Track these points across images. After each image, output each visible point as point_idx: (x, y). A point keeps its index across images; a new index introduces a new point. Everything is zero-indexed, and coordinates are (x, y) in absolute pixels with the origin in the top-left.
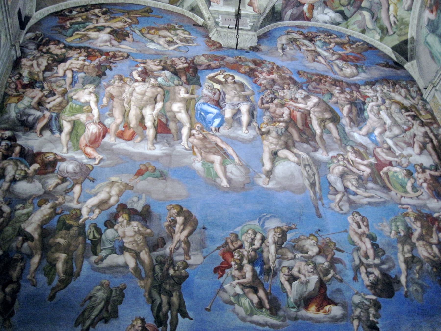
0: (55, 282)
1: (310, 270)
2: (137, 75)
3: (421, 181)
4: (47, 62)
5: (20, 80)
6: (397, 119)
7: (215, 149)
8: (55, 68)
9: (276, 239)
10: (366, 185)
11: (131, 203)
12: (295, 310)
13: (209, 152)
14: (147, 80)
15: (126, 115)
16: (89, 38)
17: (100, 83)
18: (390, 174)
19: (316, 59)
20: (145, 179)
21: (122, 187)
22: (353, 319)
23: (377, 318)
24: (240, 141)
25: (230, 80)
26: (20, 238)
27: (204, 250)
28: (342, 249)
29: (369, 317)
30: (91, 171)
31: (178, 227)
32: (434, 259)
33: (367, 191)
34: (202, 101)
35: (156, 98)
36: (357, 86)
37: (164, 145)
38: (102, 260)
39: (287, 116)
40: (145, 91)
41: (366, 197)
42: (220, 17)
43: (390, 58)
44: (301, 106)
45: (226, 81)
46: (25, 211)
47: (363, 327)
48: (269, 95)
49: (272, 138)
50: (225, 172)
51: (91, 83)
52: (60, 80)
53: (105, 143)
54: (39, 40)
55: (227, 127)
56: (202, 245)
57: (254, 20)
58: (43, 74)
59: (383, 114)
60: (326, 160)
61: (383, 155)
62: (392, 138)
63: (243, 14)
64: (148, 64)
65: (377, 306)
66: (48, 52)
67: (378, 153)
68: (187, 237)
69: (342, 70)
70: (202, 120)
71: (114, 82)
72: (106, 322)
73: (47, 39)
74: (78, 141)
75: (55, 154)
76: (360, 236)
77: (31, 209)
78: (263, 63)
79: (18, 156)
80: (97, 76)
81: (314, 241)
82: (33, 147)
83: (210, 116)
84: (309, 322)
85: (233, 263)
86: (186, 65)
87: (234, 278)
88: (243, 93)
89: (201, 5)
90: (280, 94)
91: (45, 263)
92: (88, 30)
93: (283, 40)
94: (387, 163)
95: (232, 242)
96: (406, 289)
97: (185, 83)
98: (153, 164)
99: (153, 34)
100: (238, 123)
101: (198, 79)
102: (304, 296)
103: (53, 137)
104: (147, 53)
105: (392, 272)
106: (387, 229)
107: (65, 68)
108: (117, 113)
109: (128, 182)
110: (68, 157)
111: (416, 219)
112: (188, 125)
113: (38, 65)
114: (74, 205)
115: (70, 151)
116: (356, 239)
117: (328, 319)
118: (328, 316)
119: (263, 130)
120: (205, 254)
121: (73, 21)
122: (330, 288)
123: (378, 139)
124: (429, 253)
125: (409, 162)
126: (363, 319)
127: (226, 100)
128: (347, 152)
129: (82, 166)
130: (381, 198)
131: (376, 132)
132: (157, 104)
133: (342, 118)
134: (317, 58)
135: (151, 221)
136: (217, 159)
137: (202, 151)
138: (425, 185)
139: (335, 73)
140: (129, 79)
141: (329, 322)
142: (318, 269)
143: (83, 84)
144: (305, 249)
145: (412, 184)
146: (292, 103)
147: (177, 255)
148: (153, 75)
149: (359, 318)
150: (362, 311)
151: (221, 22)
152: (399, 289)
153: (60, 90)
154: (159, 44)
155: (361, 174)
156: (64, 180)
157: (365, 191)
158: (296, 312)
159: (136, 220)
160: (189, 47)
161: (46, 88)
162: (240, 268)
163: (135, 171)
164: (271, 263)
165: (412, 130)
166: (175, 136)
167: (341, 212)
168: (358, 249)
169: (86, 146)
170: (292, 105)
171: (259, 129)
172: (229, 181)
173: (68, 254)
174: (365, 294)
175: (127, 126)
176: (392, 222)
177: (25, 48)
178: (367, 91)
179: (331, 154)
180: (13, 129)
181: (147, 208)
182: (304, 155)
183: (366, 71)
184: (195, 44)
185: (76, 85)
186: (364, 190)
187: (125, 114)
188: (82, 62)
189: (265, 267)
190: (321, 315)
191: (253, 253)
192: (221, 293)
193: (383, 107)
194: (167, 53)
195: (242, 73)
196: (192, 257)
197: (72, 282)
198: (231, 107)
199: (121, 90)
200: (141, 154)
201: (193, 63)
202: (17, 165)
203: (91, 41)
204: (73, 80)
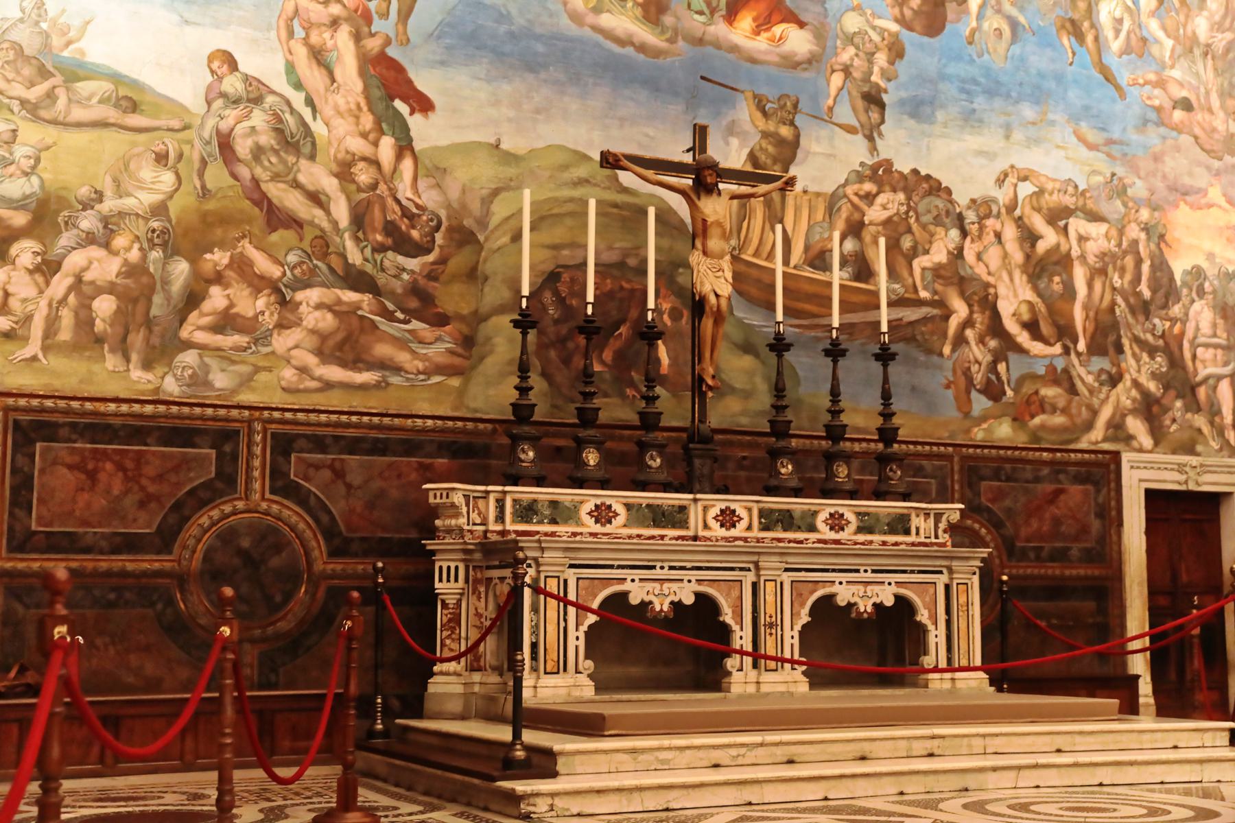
12: (702, 18)
22: (833, 71)
23: (889, 80)
29: (871, 73)
47: (849, 93)
84: (731, 56)
96: (974, 24)
117: (777, 59)
118: (778, 50)
126: (857, 74)
141: (778, 65)
149: (847, 70)
150: (857, 55)
152: (958, 20)
158: (704, 23)
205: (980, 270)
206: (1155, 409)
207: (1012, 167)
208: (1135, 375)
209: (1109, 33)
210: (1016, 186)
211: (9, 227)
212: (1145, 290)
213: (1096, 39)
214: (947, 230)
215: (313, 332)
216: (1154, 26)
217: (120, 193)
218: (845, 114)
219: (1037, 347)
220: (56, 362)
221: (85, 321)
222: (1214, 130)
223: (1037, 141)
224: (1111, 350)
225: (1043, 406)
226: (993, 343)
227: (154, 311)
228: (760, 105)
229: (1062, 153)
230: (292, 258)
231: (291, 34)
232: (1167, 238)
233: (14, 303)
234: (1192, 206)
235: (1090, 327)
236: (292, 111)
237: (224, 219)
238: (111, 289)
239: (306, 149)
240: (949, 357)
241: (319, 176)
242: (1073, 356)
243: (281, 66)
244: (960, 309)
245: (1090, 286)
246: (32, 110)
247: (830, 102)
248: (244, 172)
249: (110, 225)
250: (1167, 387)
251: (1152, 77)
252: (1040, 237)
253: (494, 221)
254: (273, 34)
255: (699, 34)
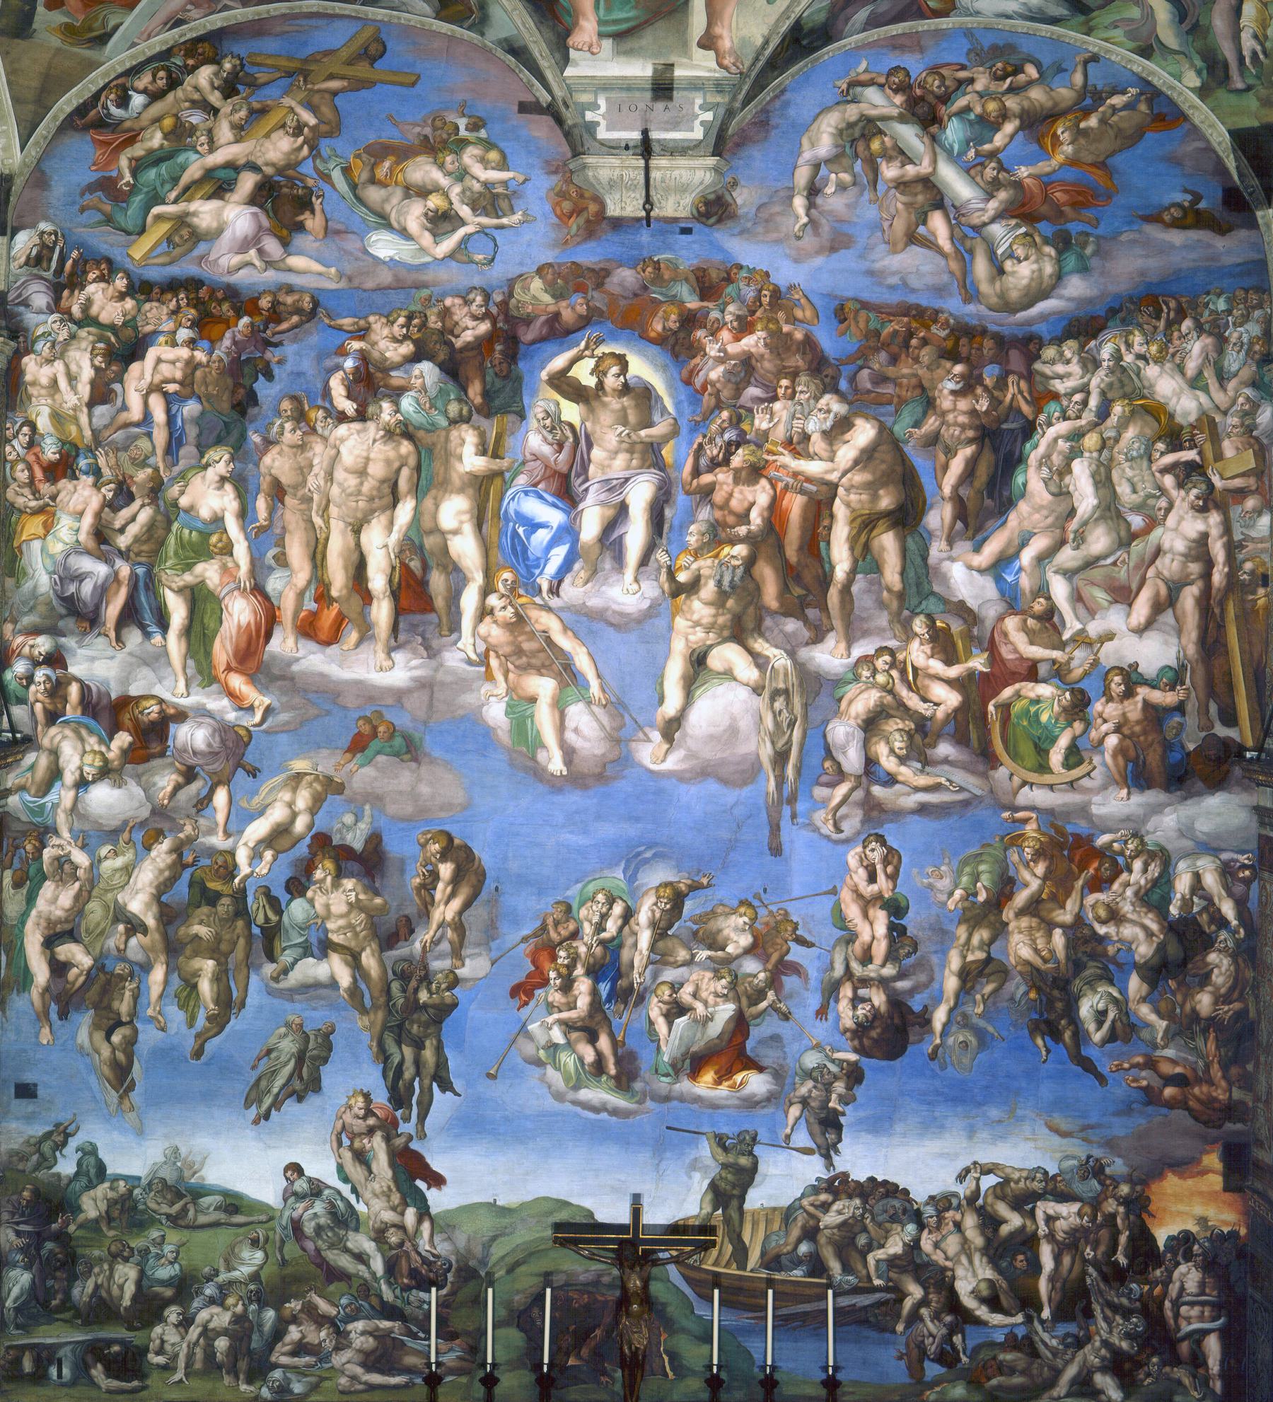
0: (201, 1022)
1: (719, 989)
2: (344, 393)
3: (1105, 728)
4: (93, 365)
5: (37, 450)
6: (1123, 489)
7: (542, 655)
8: (117, 387)
9: (658, 915)
10: (928, 752)
11: (340, 831)
13: (524, 669)
14: (371, 409)
15: (319, 557)
16: (197, 236)
17: (243, 437)
18: (1017, 708)
19: (921, 229)
20: (370, 762)
21: (318, 787)
22: (791, 1104)
23: (847, 1104)
24: (612, 625)
25: (611, 381)
26: (121, 927)
27: (493, 945)
28: (809, 938)
30: (247, 745)
31: (441, 891)
32: (1043, 967)
33: (928, 769)
34: (522, 480)
35: (395, 484)
36: (1030, 345)
37: (415, 652)
38: (285, 971)
39: (761, 515)
40: (368, 459)
41: (917, 789)
42: (602, 102)
43: (1221, 170)
44: (813, 468)
45: (600, 385)
46: (119, 862)
48: (723, 431)
49: (700, 607)
50: (561, 728)
51: (219, 442)
52: (136, 437)
53: (274, 657)
54: (54, 264)
55: (582, 574)
56: (491, 932)
57: (719, 99)
58: (90, 416)
59: (1081, 471)
60: (840, 670)
61: (1019, 640)
62: (1069, 574)
63: (680, 79)
64: (374, 337)
65: (854, 1075)
66: (88, 320)
67: (1005, 635)
68: (460, 913)
69: (1001, 272)
70: (516, 555)
71: (282, 427)
72: (300, 1099)
73: (75, 254)
74: (208, 654)
75: (161, 701)
76: (866, 904)
77: (129, 856)
78: (729, 280)
79: (79, 711)
80: (233, 407)
81: (746, 919)
82: (106, 682)
83: (542, 536)
84: (695, 1106)
85: (552, 975)
86: (484, 327)
87: (551, 1007)
88: (643, 433)
89: (536, 54)
90: (757, 422)
91: (176, 981)
92: (187, 192)
93: (823, 141)
94: (1023, 669)
95: (557, 923)
96: (938, 1041)
97: (479, 411)
98: (388, 716)
99: (385, 186)
100: (614, 558)
101: (517, 392)
102: (694, 1049)
103: (149, 647)
104: (370, 284)
105: (918, 997)
106: (945, 883)
107: (144, 384)
108: (296, 551)
109: (331, 772)
110: (191, 708)
111: (1039, 854)
112: (478, 579)
113: (72, 378)
114: (218, 841)
115: (194, 689)
116: (853, 911)
117: (736, 1102)
119: (682, 577)
120: (494, 954)
121: (138, 150)
122: (756, 1033)
123: (1025, 582)
124: (1037, 951)
125: (1096, 663)
126: (813, 1104)
127: (592, 469)
128: (909, 635)
129: (225, 731)
130: (962, 789)
131: (1027, 556)
132: (400, 506)
133: (931, 507)
134: (925, 223)
135: (383, 877)
136: (544, 686)
137: (510, 666)
138: (1112, 741)
139: (971, 294)
140: (321, 414)
141: (738, 1107)
142: (740, 989)
143: (202, 449)
144: (720, 938)
145: (1074, 739)
146: (787, 459)
147: (437, 958)
148: (386, 386)
149: (804, 1102)
151: (603, 123)
152: (921, 1041)
153: (142, 475)
154: (404, 233)
155: (928, 713)
156: (190, 775)
157: (922, 771)
159: (351, 875)
160: (496, 233)
161: (107, 472)
162: (567, 986)
163: (346, 741)
164: (636, 975)
165: (1158, 531)
166: (444, 620)
167: (835, 836)
168: (851, 938)
169: (229, 669)
170: (784, 467)
171: (671, 574)
172: (569, 754)
173: (219, 964)
174: (833, 1050)
175: (323, 597)
176: (965, 862)
177: (22, 309)
178: (1060, 368)
179: (863, 648)
180: (53, 631)
181: (375, 840)
182: (778, 658)
183: (1094, 262)
184: (517, 217)
185: (182, 452)
186: (919, 766)
187: (317, 556)
188: (184, 353)
189: (622, 983)
190: (723, 1091)
191: (598, 951)
192: (521, 1040)
193: (1091, 441)
194: (428, 276)
195: (653, 341)
196: (467, 961)
197: (233, 1021)
198: (603, 497)
199: (300, 459)
200: (359, 683)
201: (508, 318)
202: (82, 740)
203: (202, 248)
204: (171, 434)
205: (938, 1257)
206: (1127, 1366)
207: (975, 1163)
208: (1105, 1335)
209: (1091, 1027)
210: (978, 1180)
211: (163, 1299)
212: (1122, 1260)
213: (1076, 1035)
214: (903, 1226)
215: (359, 1351)
216: (1145, 1011)
217: (230, 1268)
218: (802, 1138)
219: (997, 1319)
220: (195, 1383)
221: (210, 1354)
222: (1216, 1100)
223: (1003, 1138)
224: (1079, 1316)
225: (1002, 1369)
226: (948, 1319)
227: (254, 1345)
228: (720, 1141)
229: (1031, 1144)
230: (344, 1301)
231: (340, 1144)
232: (1152, 1208)
233: (168, 1347)
234: (1182, 1176)
235: (1057, 1297)
236: (343, 1198)
237: (298, 1279)
238: (225, 1332)
239: (353, 1225)
240: (903, 1334)
241: (362, 1242)
242: (1036, 1323)
243: (333, 1167)
244: (915, 1291)
245: (1057, 1259)
246: (175, 1221)
247: (788, 1131)
248: (310, 1246)
249: (225, 1290)
250: (1142, 1348)
251: (1140, 1059)
252: (1006, 1222)
253: (493, 1259)
254: (328, 1146)
255: (664, 1092)
